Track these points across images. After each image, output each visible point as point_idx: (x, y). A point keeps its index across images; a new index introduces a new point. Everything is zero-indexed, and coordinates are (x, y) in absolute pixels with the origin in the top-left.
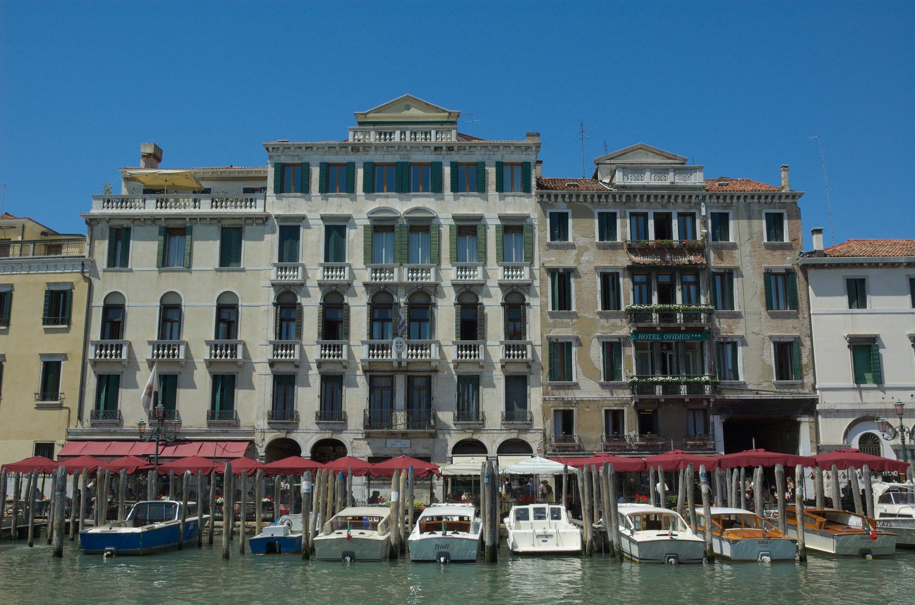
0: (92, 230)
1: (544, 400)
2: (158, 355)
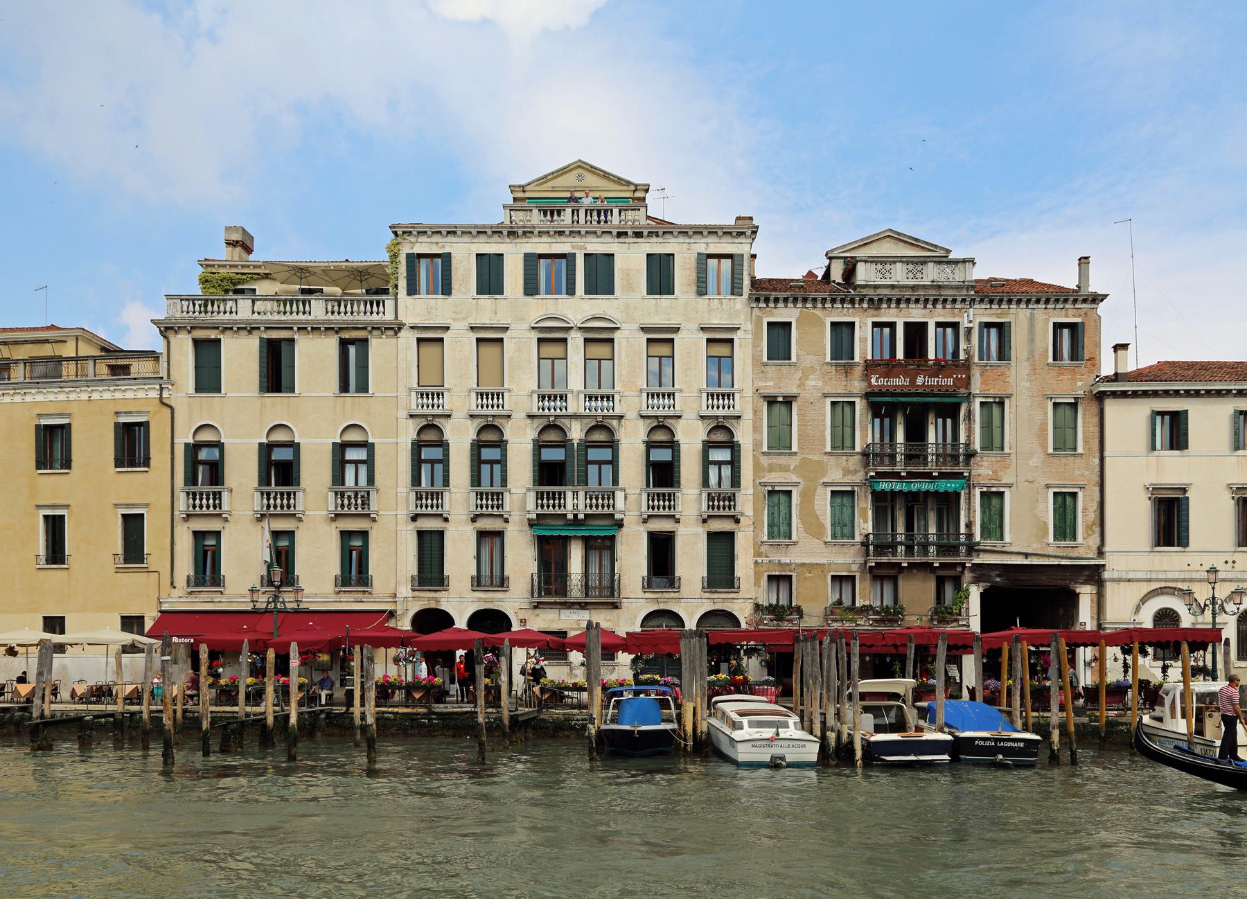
0: (168, 343)
2: (269, 507)
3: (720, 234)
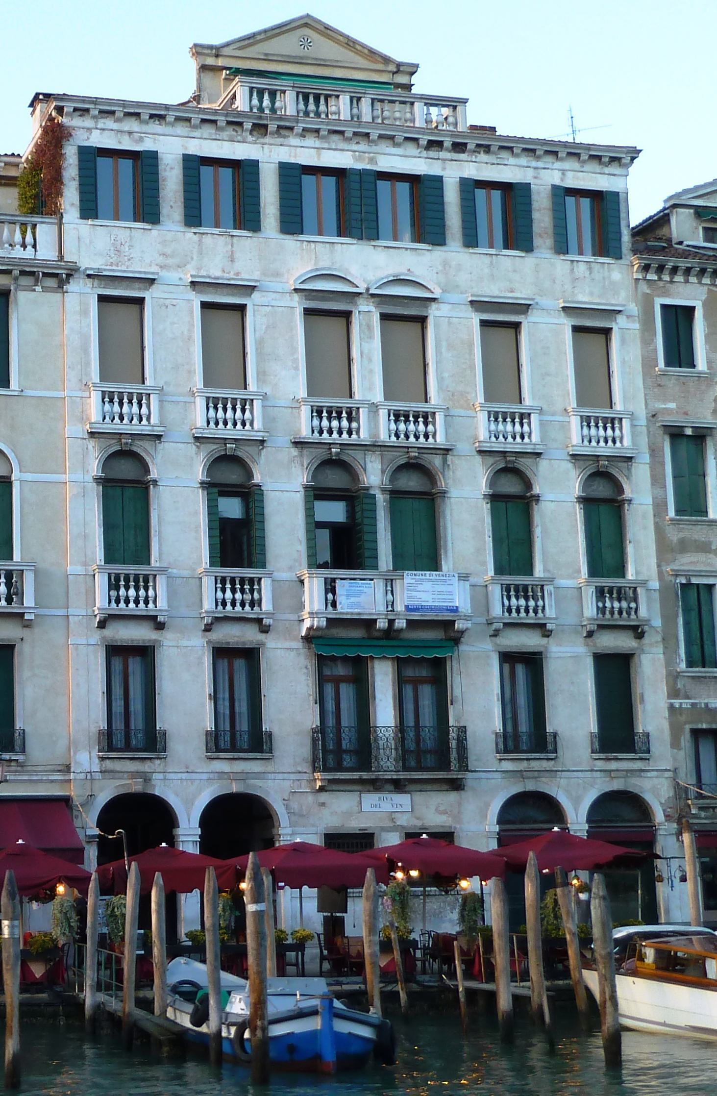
1: (671, 707)
3: (584, 157)
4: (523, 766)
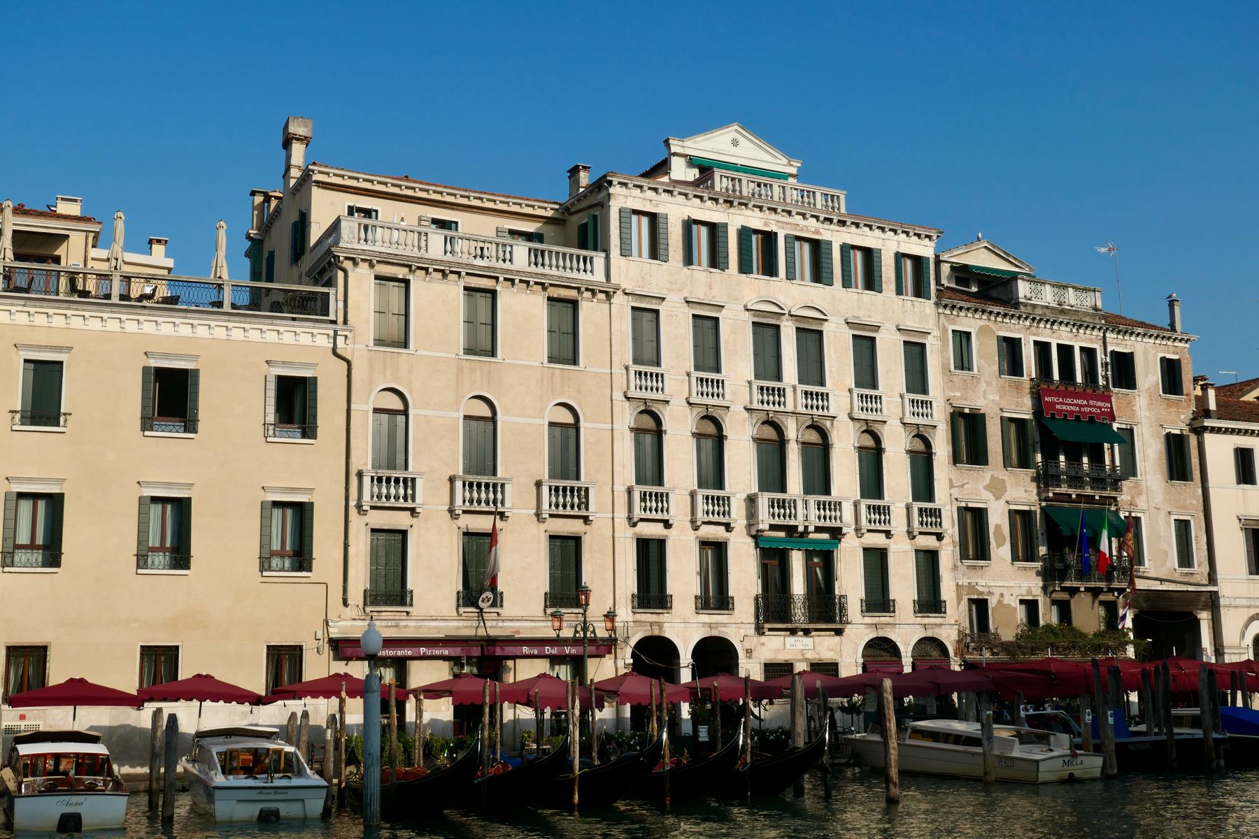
4: (876, 620)
